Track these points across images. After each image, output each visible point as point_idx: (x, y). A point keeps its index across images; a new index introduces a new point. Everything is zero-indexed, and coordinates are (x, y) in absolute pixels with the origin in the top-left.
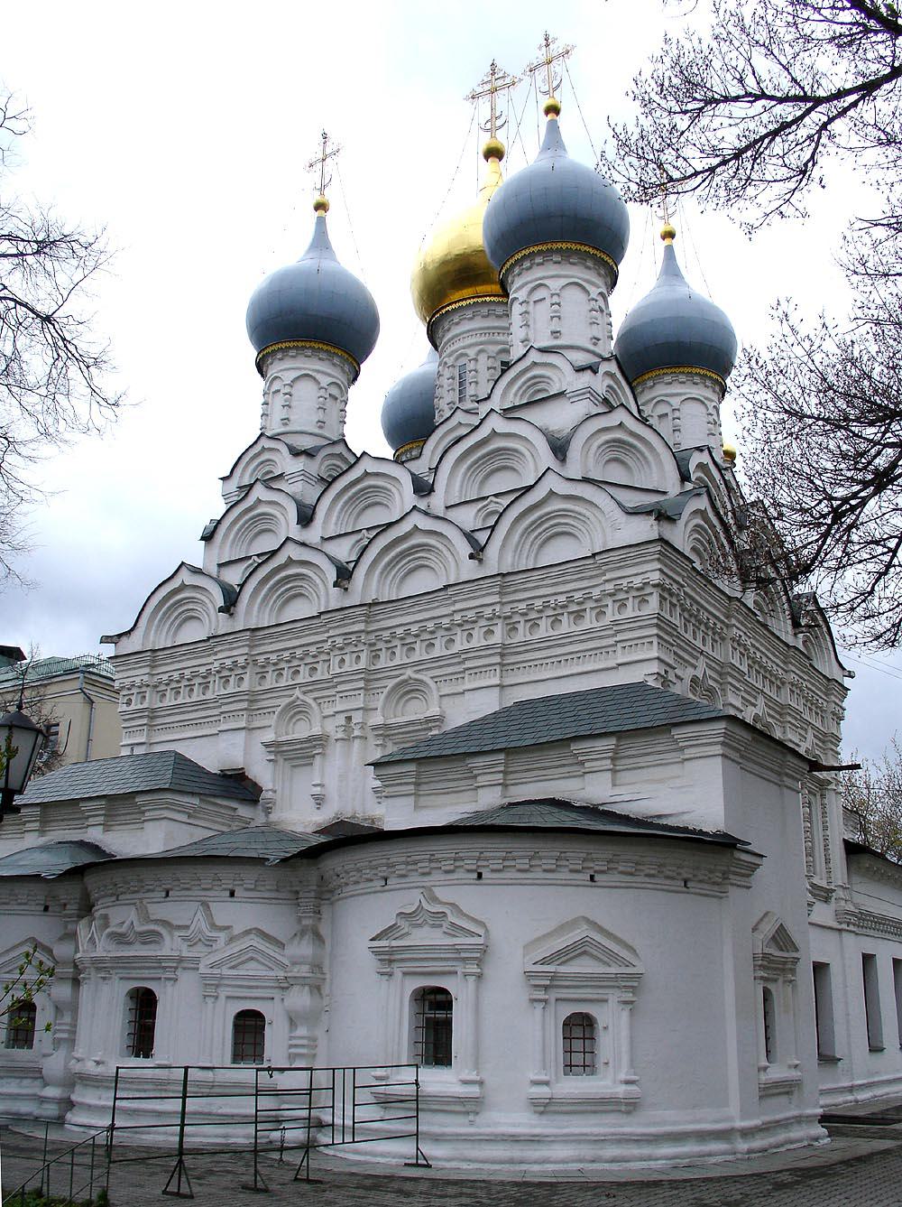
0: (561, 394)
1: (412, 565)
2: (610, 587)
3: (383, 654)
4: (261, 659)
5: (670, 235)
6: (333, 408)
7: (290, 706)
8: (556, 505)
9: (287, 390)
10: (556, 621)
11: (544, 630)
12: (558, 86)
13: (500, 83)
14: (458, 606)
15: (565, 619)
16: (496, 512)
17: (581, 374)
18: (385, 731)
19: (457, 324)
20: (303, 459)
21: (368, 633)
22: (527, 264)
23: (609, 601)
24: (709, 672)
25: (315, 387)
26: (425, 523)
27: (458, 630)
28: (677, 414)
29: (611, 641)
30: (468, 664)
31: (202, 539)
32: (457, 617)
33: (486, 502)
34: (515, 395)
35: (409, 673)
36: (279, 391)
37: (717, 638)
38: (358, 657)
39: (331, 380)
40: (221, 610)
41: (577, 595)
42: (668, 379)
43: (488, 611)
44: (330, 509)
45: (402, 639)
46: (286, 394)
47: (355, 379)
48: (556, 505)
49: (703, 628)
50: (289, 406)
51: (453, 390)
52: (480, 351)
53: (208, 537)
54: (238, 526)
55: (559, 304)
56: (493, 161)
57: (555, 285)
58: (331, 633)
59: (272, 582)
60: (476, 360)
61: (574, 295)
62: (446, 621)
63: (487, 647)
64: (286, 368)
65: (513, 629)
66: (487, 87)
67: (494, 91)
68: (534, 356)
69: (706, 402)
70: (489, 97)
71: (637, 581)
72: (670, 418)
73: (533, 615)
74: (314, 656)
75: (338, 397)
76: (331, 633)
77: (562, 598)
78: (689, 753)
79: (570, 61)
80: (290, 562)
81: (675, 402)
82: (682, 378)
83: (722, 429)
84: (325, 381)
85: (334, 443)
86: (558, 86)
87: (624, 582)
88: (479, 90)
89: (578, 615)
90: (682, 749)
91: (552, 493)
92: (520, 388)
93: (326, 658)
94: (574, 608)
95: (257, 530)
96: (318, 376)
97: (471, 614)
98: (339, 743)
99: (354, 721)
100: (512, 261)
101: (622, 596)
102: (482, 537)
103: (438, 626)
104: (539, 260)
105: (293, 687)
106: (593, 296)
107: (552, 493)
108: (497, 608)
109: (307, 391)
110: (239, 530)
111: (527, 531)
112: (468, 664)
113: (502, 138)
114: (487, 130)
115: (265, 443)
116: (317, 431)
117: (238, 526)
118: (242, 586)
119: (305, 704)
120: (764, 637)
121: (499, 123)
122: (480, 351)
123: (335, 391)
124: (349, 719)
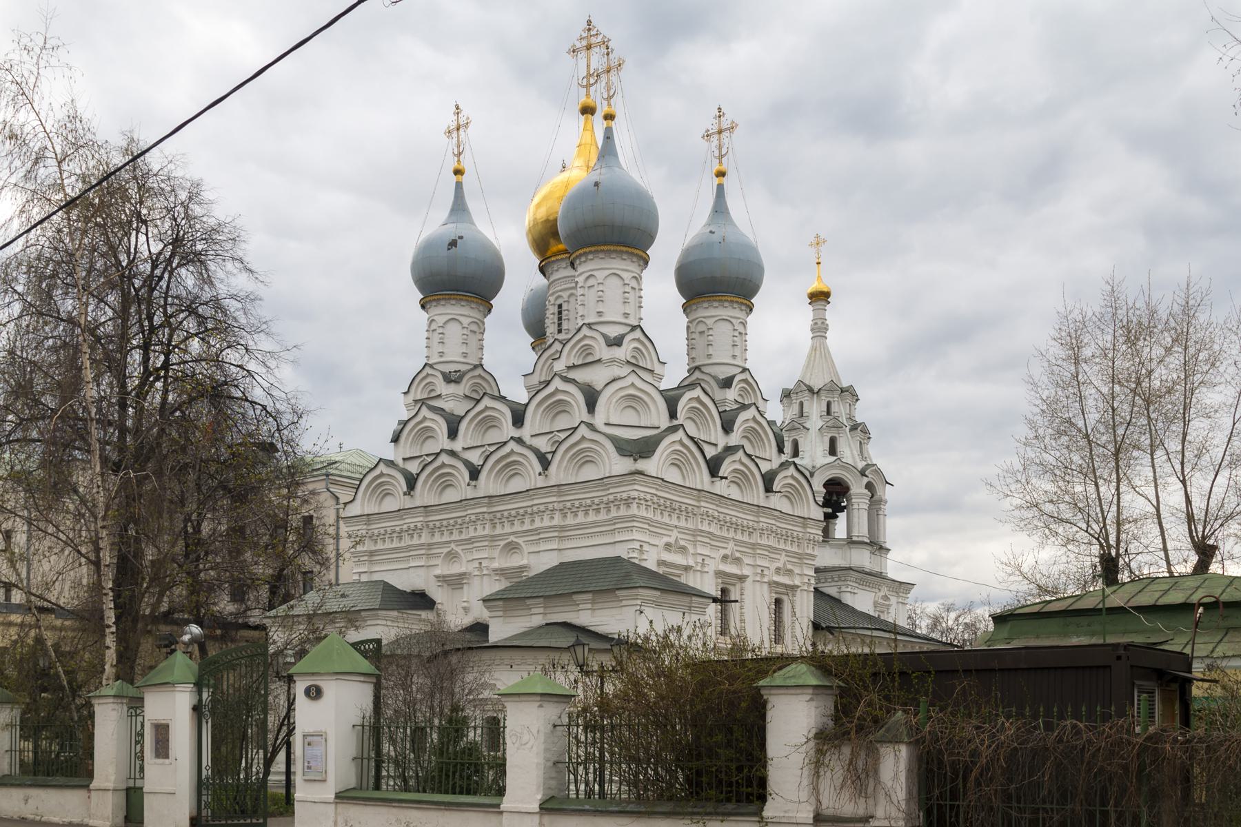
0: (599, 361)
1: (512, 473)
2: (611, 498)
3: (498, 525)
4: (431, 524)
5: (721, 174)
7: (449, 553)
8: (585, 445)
9: (441, 330)
10: (586, 513)
11: (581, 518)
13: (593, 40)
14: (536, 502)
15: (590, 512)
16: (558, 441)
17: (610, 348)
18: (502, 572)
19: (557, 270)
20: (453, 385)
21: (489, 513)
22: (583, 259)
23: (612, 505)
24: (681, 536)
25: (459, 327)
27: (536, 515)
28: (711, 332)
29: (613, 527)
30: (542, 536)
31: (391, 442)
32: (535, 508)
33: (552, 435)
34: (575, 356)
35: (512, 538)
36: (435, 330)
37: (690, 514)
38: (484, 527)
39: (470, 320)
40: (405, 494)
41: (597, 500)
42: (706, 305)
43: (550, 507)
44: (467, 429)
45: (507, 518)
46: (440, 334)
48: (585, 445)
49: (677, 512)
50: (443, 343)
51: (554, 323)
52: (572, 295)
53: (396, 439)
54: (413, 433)
55: (602, 291)
57: (600, 275)
58: (469, 512)
59: (435, 476)
61: (615, 281)
62: (529, 510)
63: (551, 527)
65: (565, 516)
66: (584, 43)
67: (589, 47)
68: (585, 331)
69: (731, 320)
71: (625, 495)
72: (706, 333)
73: (575, 510)
74: (461, 525)
76: (469, 512)
77: (589, 502)
78: (624, 603)
80: (443, 465)
81: (710, 322)
82: (716, 304)
84: (465, 321)
85: (476, 367)
86: (614, 94)
87: (618, 495)
88: (578, 45)
89: (598, 511)
90: (621, 600)
91: (583, 437)
92: (577, 352)
93: (466, 525)
94: (595, 507)
95: (425, 436)
96: (461, 319)
97: (542, 508)
98: (476, 578)
99: (483, 565)
101: (617, 503)
102: (549, 456)
103: (526, 512)
104: (590, 257)
105: (450, 542)
107: (583, 437)
108: (555, 504)
109: (454, 331)
110: (416, 434)
111: (572, 458)
112: (542, 536)
114: (583, 87)
115: (428, 370)
116: (462, 360)
117: (413, 433)
118: (418, 475)
119: (457, 553)
120: (733, 505)
123: (474, 327)
124: (480, 563)
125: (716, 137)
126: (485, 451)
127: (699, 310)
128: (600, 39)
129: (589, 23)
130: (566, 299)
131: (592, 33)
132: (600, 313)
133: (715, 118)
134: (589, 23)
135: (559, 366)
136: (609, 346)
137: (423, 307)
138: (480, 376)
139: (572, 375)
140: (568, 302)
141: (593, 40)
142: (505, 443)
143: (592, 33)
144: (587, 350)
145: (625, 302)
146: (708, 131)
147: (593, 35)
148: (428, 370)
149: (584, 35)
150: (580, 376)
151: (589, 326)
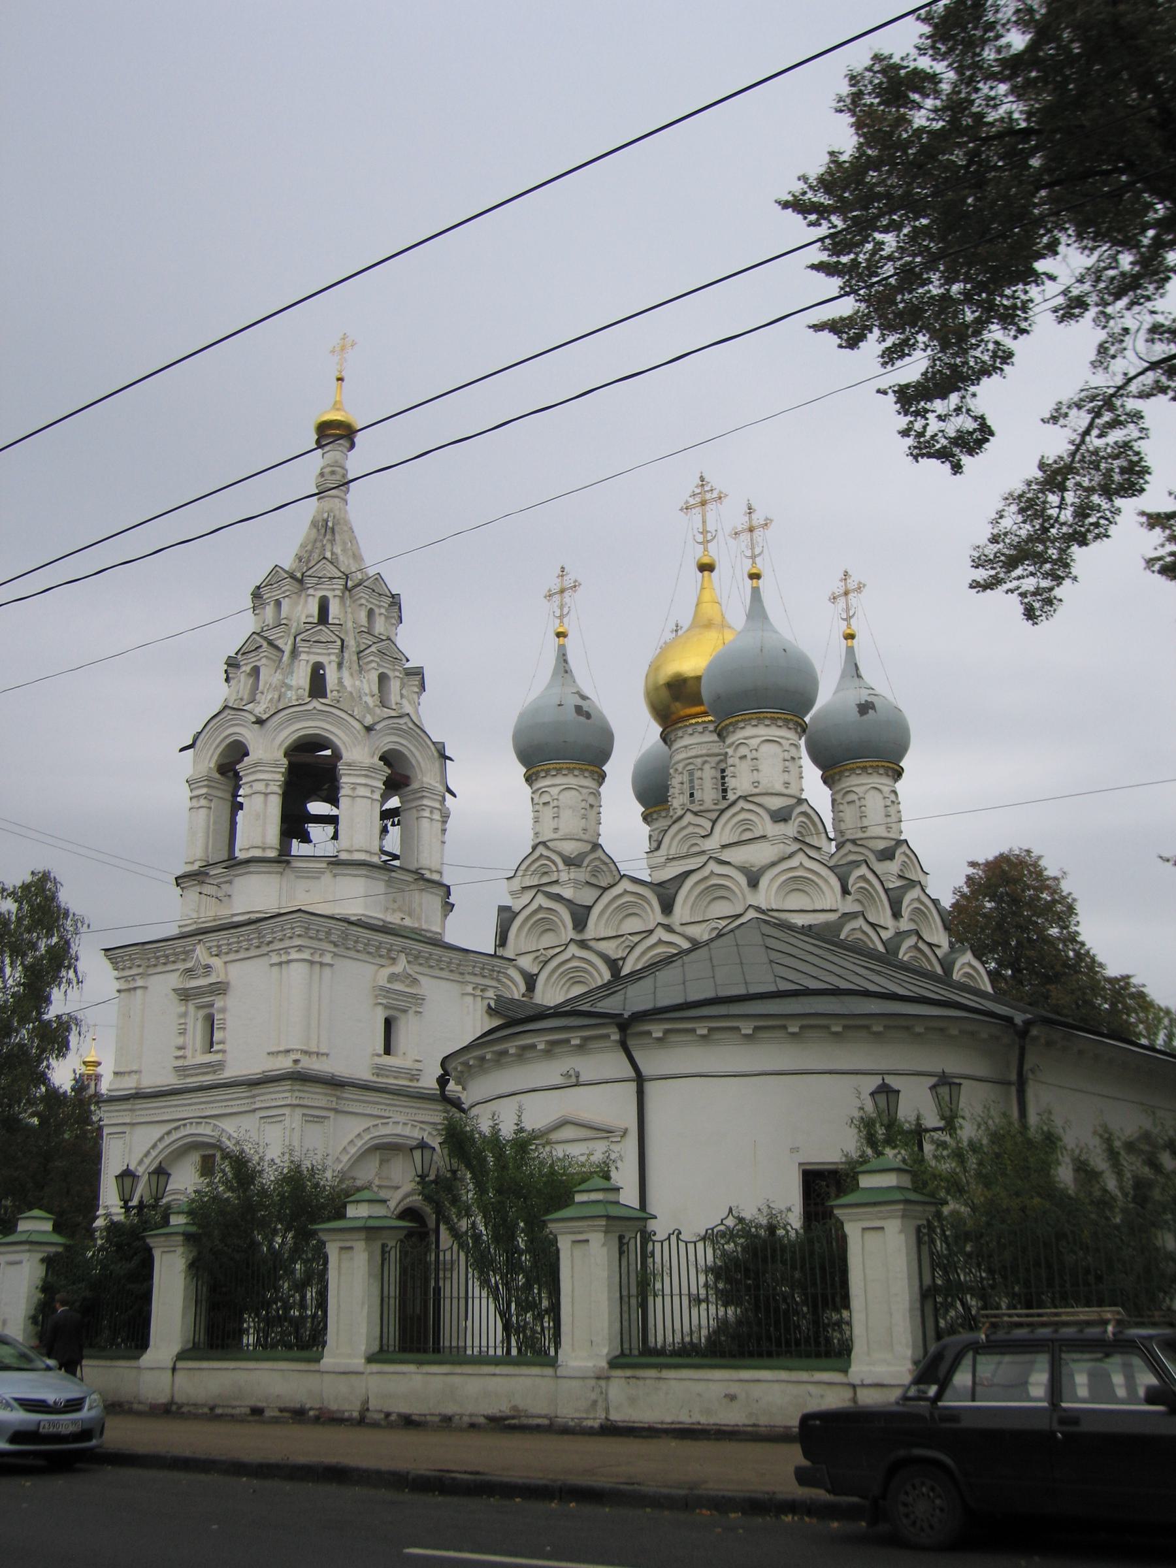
0: (764, 837)
6: (592, 814)
12: (760, 554)
26: (667, 937)
36: (549, 803)
47: (604, 779)
56: (706, 560)
60: (701, 769)
64: (553, 785)
66: (698, 499)
67: (703, 503)
70: (698, 510)
75: (593, 806)
79: (770, 532)
83: (901, 807)
88: (692, 501)
100: (727, 722)
106: (787, 747)
113: (714, 553)
121: (709, 537)
122: (705, 762)
123: (591, 800)
125: (843, 599)
126: (624, 942)
127: (844, 779)
128: (715, 495)
129: (702, 479)
130: (699, 766)
131: (707, 488)
132: (756, 784)
133: (841, 580)
134: (702, 479)
135: (711, 844)
136: (776, 822)
137: (527, 780)
138: (599, 858)
139: (726, 855)
140: (701, 769)
141: (708, 496)
142: (651, 932)
143: (707, 488)
144: (747, 825)
145: (784, 771)
146: (834, 593)
147: (708, 491)
148: (541, 850)
149: (698, 491)
150: (736, 856)
151: (744, 798)
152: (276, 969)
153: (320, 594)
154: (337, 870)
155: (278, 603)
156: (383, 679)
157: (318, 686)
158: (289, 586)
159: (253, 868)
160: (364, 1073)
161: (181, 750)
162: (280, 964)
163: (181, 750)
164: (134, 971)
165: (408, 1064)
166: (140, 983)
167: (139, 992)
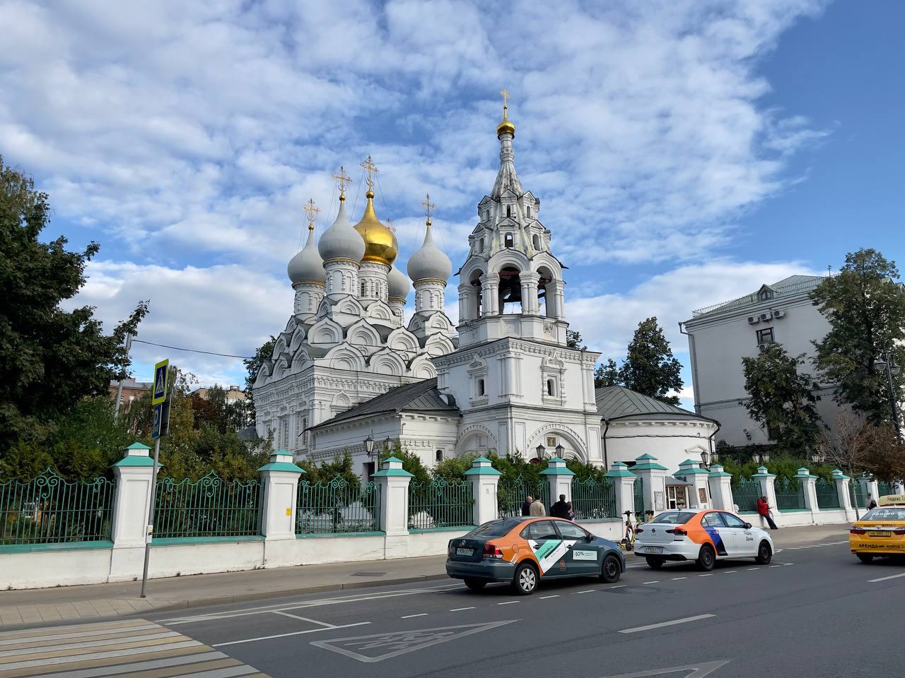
152: (499, 362)
153: (506, 204)
154: (522, 320)
155: (488, 211)
156: (535, 237)
157: (509, 244)
158: (493, 203)
159: (488, 320)
160: (539, 404)
161: (455, 275)
162: (501, 360)
163: (455, 275)
164: (444, 367)
165: (560, 399)
166: (446, 371)
167: (446, 375)
